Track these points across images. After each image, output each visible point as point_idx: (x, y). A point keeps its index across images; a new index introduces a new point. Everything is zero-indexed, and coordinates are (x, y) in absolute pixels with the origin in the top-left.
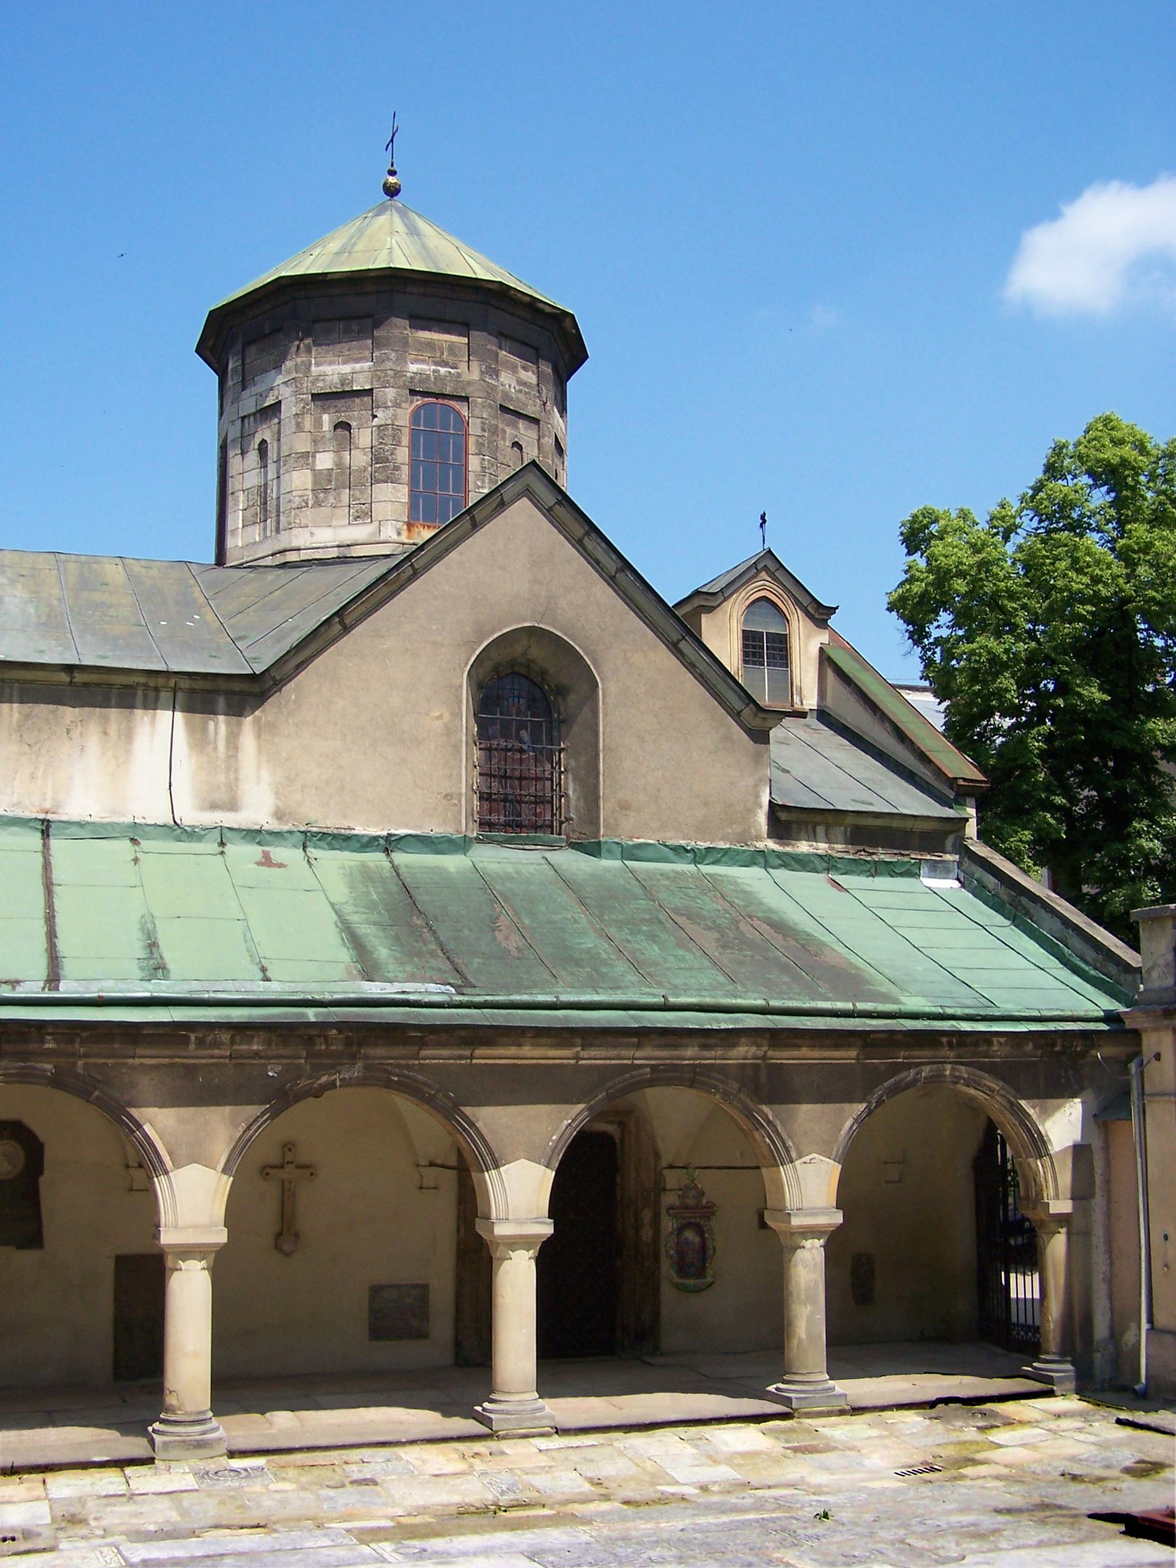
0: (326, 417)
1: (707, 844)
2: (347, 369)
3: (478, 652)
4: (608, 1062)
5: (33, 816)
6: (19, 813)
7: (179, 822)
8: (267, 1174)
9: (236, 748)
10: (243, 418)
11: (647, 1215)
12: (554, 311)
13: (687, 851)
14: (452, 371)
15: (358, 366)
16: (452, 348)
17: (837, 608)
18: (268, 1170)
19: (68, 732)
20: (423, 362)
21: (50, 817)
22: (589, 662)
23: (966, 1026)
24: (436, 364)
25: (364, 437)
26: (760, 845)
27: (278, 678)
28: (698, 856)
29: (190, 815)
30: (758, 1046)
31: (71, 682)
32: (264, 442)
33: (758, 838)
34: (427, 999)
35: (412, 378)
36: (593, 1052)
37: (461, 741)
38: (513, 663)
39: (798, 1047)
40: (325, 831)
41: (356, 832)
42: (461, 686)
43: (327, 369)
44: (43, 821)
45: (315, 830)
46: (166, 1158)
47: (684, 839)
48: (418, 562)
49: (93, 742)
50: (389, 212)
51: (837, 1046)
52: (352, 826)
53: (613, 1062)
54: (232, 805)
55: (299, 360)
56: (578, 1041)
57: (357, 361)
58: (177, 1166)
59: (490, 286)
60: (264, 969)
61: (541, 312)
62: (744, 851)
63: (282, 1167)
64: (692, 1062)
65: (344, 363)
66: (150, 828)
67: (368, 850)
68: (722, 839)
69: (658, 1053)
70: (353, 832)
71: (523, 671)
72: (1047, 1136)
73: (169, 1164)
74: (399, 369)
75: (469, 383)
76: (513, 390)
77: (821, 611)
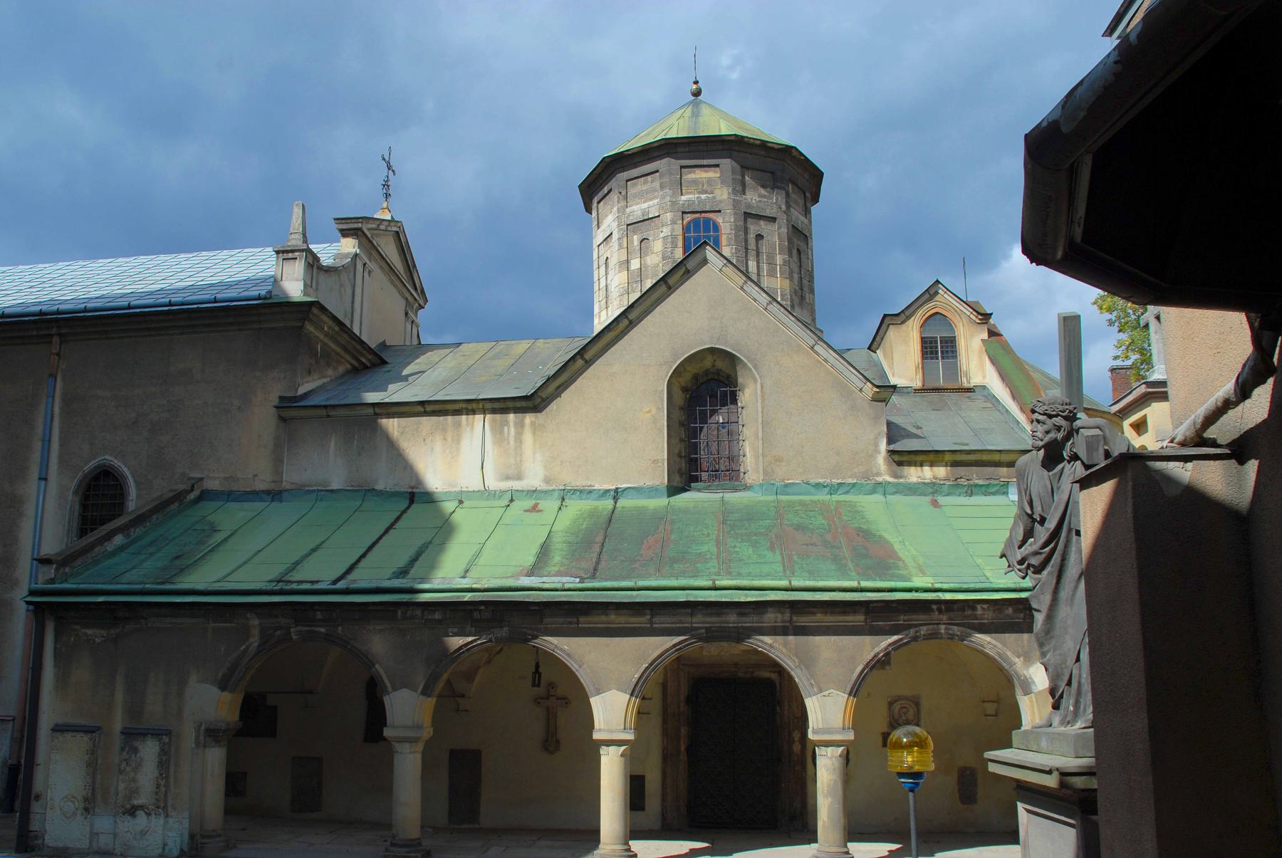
0: (635, 237)
1: (839, 481)
2: (645, 205)
3: (674, 368)
4: (674, 625)
5: (406, 490)
6: (398, 489)
7: (487, 488)
8: (539, 703)
9: (521, 442)
10: (599, 246)
12: (780, 147)
13: (824, 487)
14: (709, 196)
15: (651, 203)
16: (710, 181)
17: (991, 314)
18: (539, 700)
19: (424, 440)
20: (690, 193)
21: (414, 490)
22: (751, 366)
23: (948, 596)
24: (699, 193)
25: (658, 246)
26: (880, 479)
27: (544, 396)
28: (833, 489)
29: (493, 484)
30: (783, 613)
31: (425, 411)
32: (607, 258)
33: (878, 474)
34: (546, 586)
35: (683, 204)
36: (663, 619)
37: (664, 425)
38: (707, 372)
39: (814, 614)
40: (576, 488)
42: (663, 391)
43: (635, 208)
44: (411, 493)
45: (569, 488)
46: (389, 685)
47: (822, 478)
48: (632, 316)
49: (438, 446)
51: (844, 613)
53: (678, 625)
54: (519, 477)
55: (619, 205)
56: (648, 611)
58: (395, 689)
59: (730, 138)
61: (772, 149)
63: (548, 698)
64: (736, 625)
65: (644, 202)
66: (470, 494)
67: (603, 498)
69: (708, 619)
71: (716, 377)
72: (1031, 678)
73: (390, 689)
74: (674, 200)
75: (721, 202)
76: (754, 201)
77: (980, 317)
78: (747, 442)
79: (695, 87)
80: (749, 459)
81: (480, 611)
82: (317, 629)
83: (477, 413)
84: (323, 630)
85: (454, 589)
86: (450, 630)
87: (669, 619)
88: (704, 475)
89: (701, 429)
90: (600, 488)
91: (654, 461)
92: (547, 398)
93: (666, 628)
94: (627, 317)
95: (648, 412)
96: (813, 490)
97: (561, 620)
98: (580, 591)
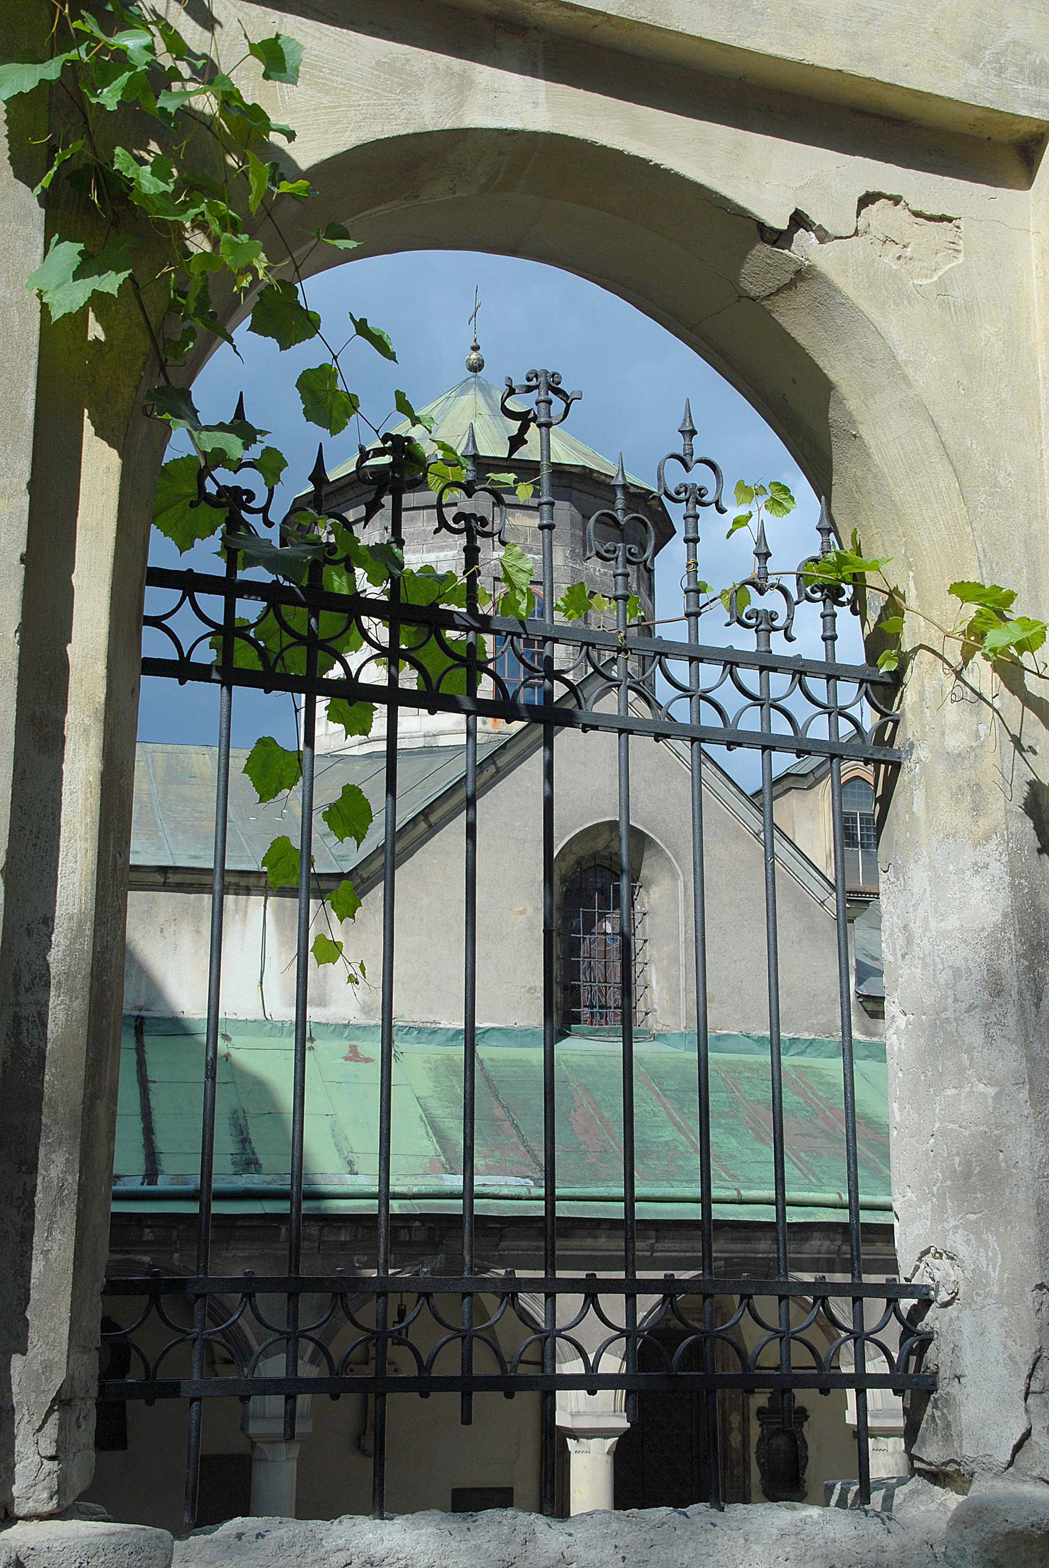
1: (791, 1035)
4: (682, 1254)
7: (269, 1017)
11: (735, 1419)
12: (639, 491)
19: (162, 931)
21: (144, 1013)
22: (670, 855)
27: (365, 876)
30: (832, 1240)
31: (165, 882)
34: (505, 1191)
36: (668, 1244)
38: (595, 856)
39: (873, 1242)
40: (411, 1024)
41: (441, 1026)
44: (138, 1017)
50: (472, 391)
52: (437, 1020)
53: (687, 1254)
56: (652, 1233)
57: (441, 549)
59: (574, 470)
60: (350, 1163)
62: (830, 1042)
64: (766, 1255)
66: (240, 1023)
67: (454, 1043)
68: (807, 1030)
69: (733, 1246)
70: (438, 1026)
71: (606, 864)
78: (653, 967)
79: (474, 356)
80: (656, 995)
81: (410, 1228)
82: (137, 1258)
83: (253, 892)
84: (146, 1259)
85: (367, 1193)
86: (355, 1258)
87: (677, 1245)
88: (585, 1012)
89: (584, 939)
90: (449, 1026)
91: (531, 988)
92: (368, 878)
93: (680, 1259)
94: (494, 763)
95: (521, 913)
96: (755, 1046)
97: (524, 1244)
98: (578, 1200)
